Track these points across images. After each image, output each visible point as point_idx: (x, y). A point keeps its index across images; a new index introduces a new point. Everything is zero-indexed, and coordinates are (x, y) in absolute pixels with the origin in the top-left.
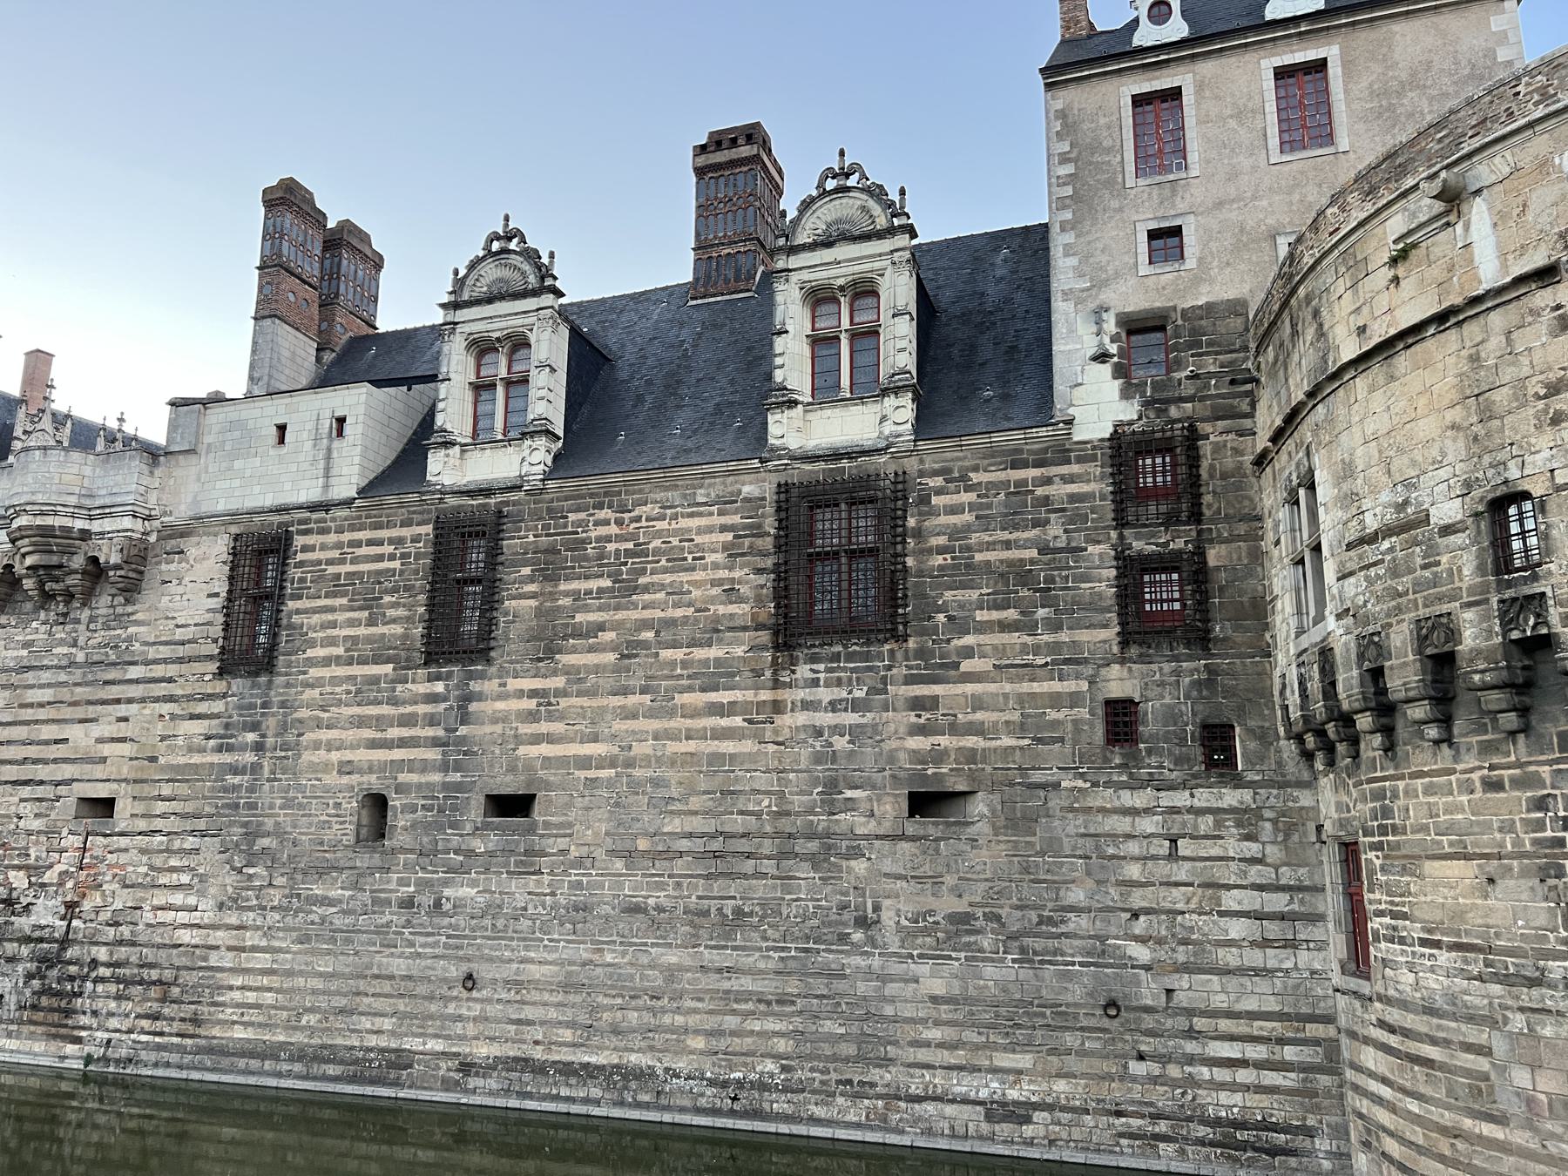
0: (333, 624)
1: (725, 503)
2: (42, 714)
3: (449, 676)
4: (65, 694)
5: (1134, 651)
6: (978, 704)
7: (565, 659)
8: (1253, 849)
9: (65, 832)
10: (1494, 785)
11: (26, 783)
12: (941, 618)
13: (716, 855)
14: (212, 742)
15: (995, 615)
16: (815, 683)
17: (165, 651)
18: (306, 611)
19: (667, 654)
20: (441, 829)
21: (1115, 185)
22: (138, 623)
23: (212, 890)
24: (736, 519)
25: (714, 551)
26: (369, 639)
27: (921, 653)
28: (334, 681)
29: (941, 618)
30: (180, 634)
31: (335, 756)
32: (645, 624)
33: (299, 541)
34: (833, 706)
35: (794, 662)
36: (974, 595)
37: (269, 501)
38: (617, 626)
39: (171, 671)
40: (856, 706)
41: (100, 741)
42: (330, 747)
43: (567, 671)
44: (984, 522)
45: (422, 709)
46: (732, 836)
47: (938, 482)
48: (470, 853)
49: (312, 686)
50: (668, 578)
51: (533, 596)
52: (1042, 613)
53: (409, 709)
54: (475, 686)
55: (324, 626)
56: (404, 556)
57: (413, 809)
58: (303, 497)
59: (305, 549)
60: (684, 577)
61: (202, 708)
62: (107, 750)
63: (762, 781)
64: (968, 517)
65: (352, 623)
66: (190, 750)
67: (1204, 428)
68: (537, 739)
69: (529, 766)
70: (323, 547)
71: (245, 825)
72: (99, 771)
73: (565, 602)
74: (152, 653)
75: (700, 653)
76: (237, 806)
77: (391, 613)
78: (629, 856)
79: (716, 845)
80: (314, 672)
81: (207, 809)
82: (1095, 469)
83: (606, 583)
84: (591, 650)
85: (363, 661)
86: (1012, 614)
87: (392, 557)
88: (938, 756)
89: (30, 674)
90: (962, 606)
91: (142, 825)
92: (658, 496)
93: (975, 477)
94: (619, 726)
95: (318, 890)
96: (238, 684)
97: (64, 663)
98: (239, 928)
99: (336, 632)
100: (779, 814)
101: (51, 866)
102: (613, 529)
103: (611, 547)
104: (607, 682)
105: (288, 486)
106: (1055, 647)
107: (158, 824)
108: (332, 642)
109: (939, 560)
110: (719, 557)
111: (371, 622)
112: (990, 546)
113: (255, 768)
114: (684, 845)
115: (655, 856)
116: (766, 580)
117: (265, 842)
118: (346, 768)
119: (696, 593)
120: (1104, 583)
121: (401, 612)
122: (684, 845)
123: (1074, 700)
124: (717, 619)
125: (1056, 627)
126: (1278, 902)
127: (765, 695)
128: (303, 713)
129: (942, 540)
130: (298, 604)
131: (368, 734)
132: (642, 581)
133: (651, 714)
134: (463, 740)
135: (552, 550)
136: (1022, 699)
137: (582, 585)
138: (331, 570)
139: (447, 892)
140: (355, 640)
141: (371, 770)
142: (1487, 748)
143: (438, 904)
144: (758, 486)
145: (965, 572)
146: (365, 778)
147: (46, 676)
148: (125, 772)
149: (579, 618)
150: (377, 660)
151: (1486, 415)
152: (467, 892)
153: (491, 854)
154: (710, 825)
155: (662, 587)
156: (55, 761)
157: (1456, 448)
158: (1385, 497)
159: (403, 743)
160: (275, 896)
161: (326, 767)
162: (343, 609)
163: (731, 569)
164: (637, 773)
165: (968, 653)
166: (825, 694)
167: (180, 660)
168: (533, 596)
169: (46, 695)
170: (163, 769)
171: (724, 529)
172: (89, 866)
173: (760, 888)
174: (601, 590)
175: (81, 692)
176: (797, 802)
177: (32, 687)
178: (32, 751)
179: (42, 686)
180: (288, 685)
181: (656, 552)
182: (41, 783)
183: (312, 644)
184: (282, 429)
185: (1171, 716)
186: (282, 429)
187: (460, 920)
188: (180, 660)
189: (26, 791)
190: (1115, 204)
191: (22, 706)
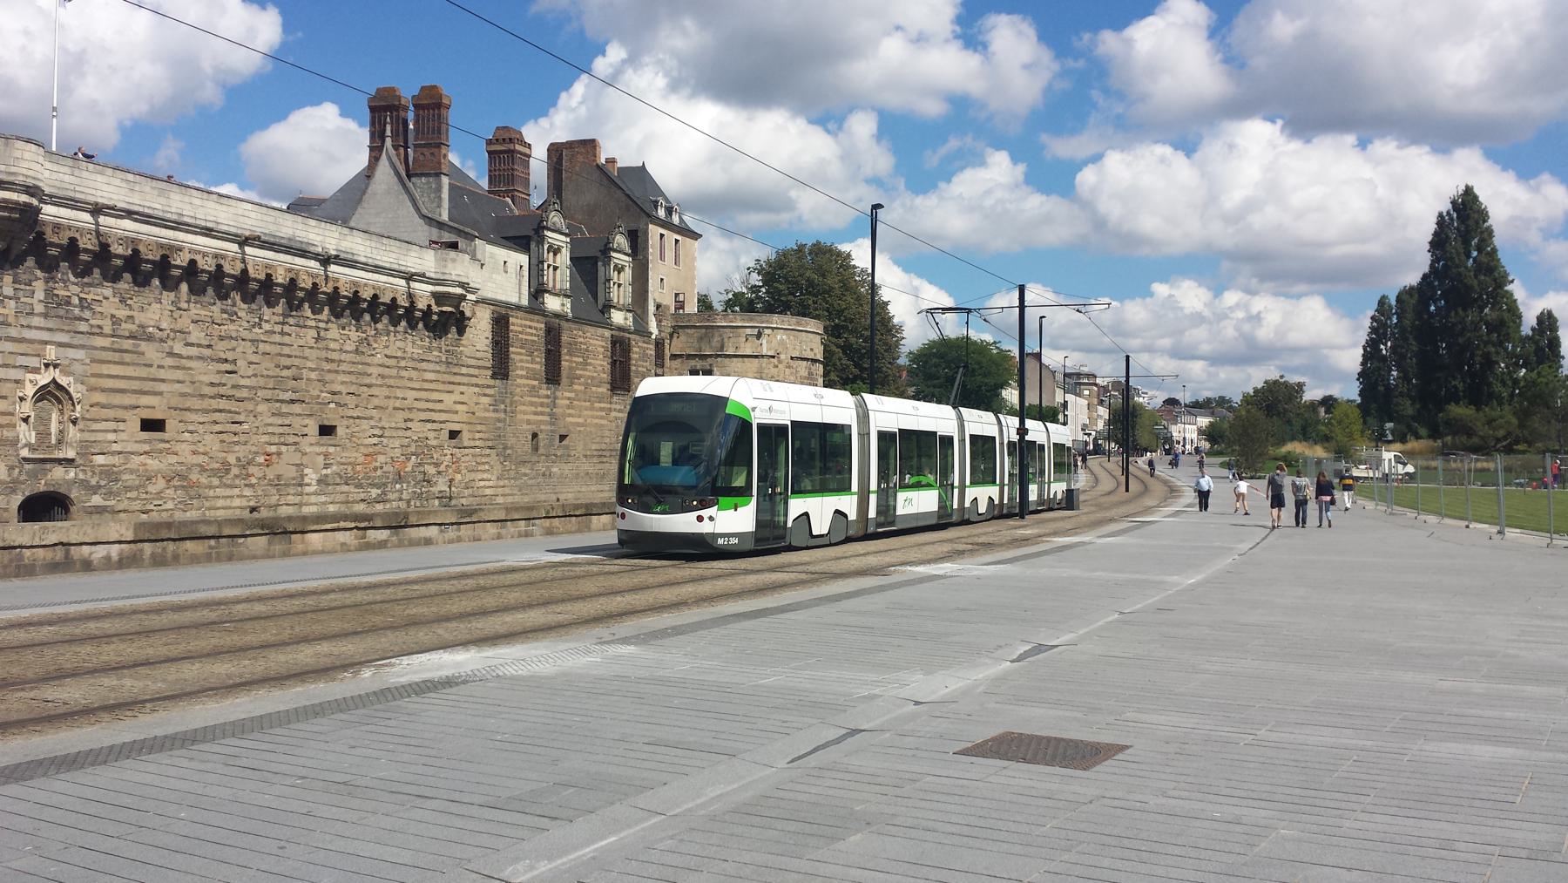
4: (440, 377)
11: (428, 421)
13: (601, 456)
17: (473, 362)
19: (594, 389)
22: (463, 346)
23: (495, 472)
24: (604, 344)
28: (524, 385)
30: (478, 355)
32: (589, 377)
39: (476, 372)
41: (455, 403)
50: (593, 361)
62: (459, 407)
65: (527, 362)
68: (570, 415)
72: (456, 418)
78: (586, 456)
83: (581, 360)
84: (580, 384)
89: (425, 363)
96: (498, 382)
97: (438, 360)
98: (503, 487)
103: (582, 346)
107: (478, 443)
114: (595, 453)
118: (529, 422)
127: (609, 406)
131: (533, 409)
132: (589, 361)
147: (431, 366)
149: (577, 372)
160: (512, 473)
163: (604, 361)
166: (618, 407)
167: (479, 367)
170: (477, 418)
171: (603, 347)
175: (448, 378)
177: (425, 370)
178: (430, 405)
179: (430, 371)
180: (512, 385)
182: (434, 422)
184: (505, 262)
186: (505, 262)
187: (555, 480)
188: (479, 367)
189: (429, 426)
191: (424, 381)
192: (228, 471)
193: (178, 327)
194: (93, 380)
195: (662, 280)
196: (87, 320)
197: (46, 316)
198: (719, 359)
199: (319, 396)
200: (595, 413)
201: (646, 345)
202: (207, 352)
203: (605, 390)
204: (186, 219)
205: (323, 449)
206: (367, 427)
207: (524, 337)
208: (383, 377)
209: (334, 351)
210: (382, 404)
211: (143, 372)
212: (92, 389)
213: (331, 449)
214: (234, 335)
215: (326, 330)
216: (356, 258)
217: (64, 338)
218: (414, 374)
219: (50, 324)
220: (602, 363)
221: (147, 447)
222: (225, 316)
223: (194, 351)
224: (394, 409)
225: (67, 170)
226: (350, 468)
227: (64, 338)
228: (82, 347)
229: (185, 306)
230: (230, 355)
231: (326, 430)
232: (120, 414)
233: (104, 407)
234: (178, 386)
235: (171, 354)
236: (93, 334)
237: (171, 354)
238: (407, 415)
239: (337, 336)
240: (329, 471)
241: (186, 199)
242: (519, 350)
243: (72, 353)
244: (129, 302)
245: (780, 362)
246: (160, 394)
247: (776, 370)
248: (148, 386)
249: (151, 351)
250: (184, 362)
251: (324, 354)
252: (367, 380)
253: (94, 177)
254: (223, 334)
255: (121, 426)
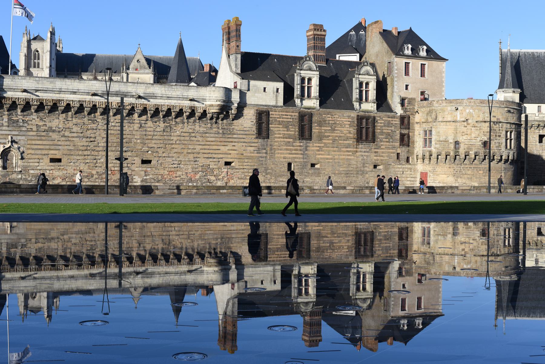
0: (280, 131)
1: (349, 117)
2: (212, 143)
3: (303, 142)
4: (218, 139)
5: (401, 146)
6: (383, 153)
7: (324, 141)
8: (411, 173)
9: (223, 168)
10: (450, 168)
12: (379, 140)
14: (255, 152)
15: (386, 140)
16: (362, 148)
18: (274, 127)
19: (340, 142)
20: (304, 169)
21: (402, 76)
24: (350, 120)
25: (347, 125)
26: (287, 134)
27: (376, 145)
28: (281, 141)
29: (379, 140)
30: (245, 129)
31: (282, 156)
32: (337, 136)
33: (271, 113)
34: (365, 152)
35: (359, 144)
36: (383, 137)
37: (264, 104)
38: (332, 136)
39: (244, 136)
40: (367, 152)
41: (228, 150)
42: (281, 154)
43: (324, 143)
44: (385, 126)
45: (299, 148)
46: (349, 171)
47: (379, 118)
48: (308, 173)
49: (277, 142)
50: (340, 129)
51: (317, 129)
52: (391, 140)
53: (296, 148)
54: (308, 144)
55: (278, 131)
56: (293, 119)
57: (298, 165)
58: (271, 104)
59: (272, 114)
60: (342, 129)
61: (253, 145)
62: (231, 152)
63: (354, 163)
64: (383, 125)
65: (284, 131)
66: (251, 153)
67: (410, 116)
68: (319, 154)
69: (318, 159)
70: (276, 115)
71: (265, 168)
72: (229, 156)
73: (323, 131)
74: (239, 132)
75: (345, 142)
76: (262, 164)
77: (291, 129)
78: (335, 174)
79: (347, 172)
80: (276, 139)
81: (256, 165)
82: (398, 120)
83: (330, 128)
84: (328, 140)
85: (286, 138)
86: (387, 140)
87: (290, 119)
88: (378, 160)
90: (382, 138)
91: (242, 167)
92: (338, 114)
93: (384, 119)
94: (333, 153)
95: (281, 179)
96: (260, 140)
97: (216, 132)
99: (280, 132)
100: (356, 168)
101: (220, 175)
102: (330, 119)
103: (331, 122)
104: (331, 145)
105: (268, 101)
106: (392, 145)
108: (280, 134)
109: (379, 131)
110: (348, 126)
111: (287, 131)
112: (385, 129)
113: (266, 157)
114: (343, 172)
115: (339, 174)
116: (355, 131)
117: (269, 171)
118: (284, 158)
119: (344, 132)
120: (398, 137)
121: (293, 129)
122: (343, 172)
123: (394, 153)
124: (348, 137)
125: (392, 142)
126: (413, 179)
127: (355, 150)
128: (275, 147)
129: (379, 128)
130: (272, 126)
132: (336, 129)
133: (338, 151)
134: (306, 154)
135: (320, 121)
136: (388, 152)
137: (326, 128)
138: (278, 119)
139: (305, 180)
140: (285, 134)
141: (290, 158)
142: (449, 164)
143: (304, 182)
144: (354, 114)
145: (382, 133)
146: (288, 160)
147: (212, 135)
148: (236, 156)
149: (326, 134)
150: (289, 138)
151: (456, 133)
152: (308, 179)
153: (312, 173)
154: (347, 169)
155: (339, 130)
156: (218, 154)
157: (453, 135)
158: (444, 137)
159: (295, 154)
161: (281, 157)
162: (281, 128)
164: (336, 161)
165: (382, 145)
166: (363, 150)
167: (246, 135)
168: (317, 129)
169: (213, 139)
171: (349, 121)
172: (229, 175)
173: (354, 179)
174: (329, 130)
175: (222, 139)
176: (359, 166)
177: (209, 137)
178: (211, 151)
179: (211, 137)
180: (271, 141)
181: (338, 124)
183: (276, 134)
184: (265, 88)
185: (404, 156)
186: (265, 88)
188: (246, 135)
189: (211, 160)
190: (402, 79)
192: (92, 176)
193: (68, 126)
194: (28, 146)
195: (407, 86)
196: (26, 127)
197: (8, 126)
198: (435, 124)
199: (141, 149)
200: (342, 153)
201: (390, 119)
202: (81, 135)
203: (351, 142)
204: (63, 90)
205: (145, 169)
206: (171, 161)
207: (281, 120)
208: (180, 140)
209: (151, 131)
210: (179, 151)
211: (51, 143)
212: (28, 149)
213: (149, 169)
214: (95, 128)
215: (145, 124)
216: (155, 95)
217: (16, 133)
218: (200, 139)
219: (10, 129)
220: (349, 129)
221: (53, 168)
222: (91, 122)
223: (75, 135)
224: (187, 153)
225: (10, 80)
226: (160, 177)
227: (16, 133)
228: (24, 135)
229: (69, 119)
230: (92, 135)
231: (145, 162)
232: (40, 157)
233: (32, 154)
234: (67, 147)
235: (64, 136)
236: (29, 131)
237: (64, 136)
238: (195, 155)
239: (152, 126)
240: (148, 177)
241: (64, 83)
242: (278, 126)
243: (19, 138)
244: (44, 120)
245: (468, 124)
246: (59, 150)
247: (466, 128)
248: (53, 147)
249: (54, 136)
250: (70, 139)
251: (144, 133)
252: (171, 142)
253: (21, 81)
254: (89, 128)
255: (41, 161)
